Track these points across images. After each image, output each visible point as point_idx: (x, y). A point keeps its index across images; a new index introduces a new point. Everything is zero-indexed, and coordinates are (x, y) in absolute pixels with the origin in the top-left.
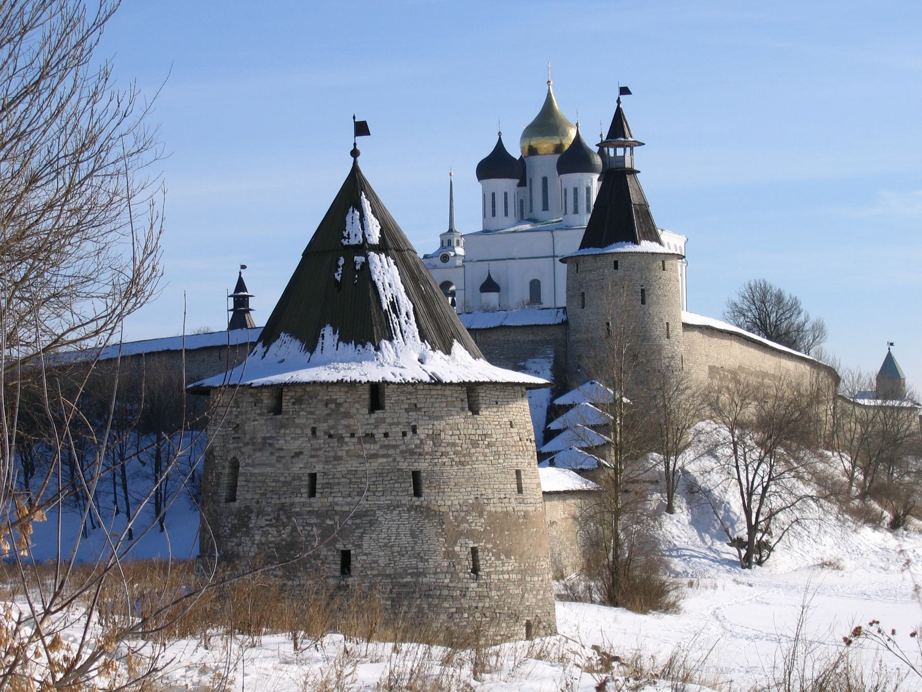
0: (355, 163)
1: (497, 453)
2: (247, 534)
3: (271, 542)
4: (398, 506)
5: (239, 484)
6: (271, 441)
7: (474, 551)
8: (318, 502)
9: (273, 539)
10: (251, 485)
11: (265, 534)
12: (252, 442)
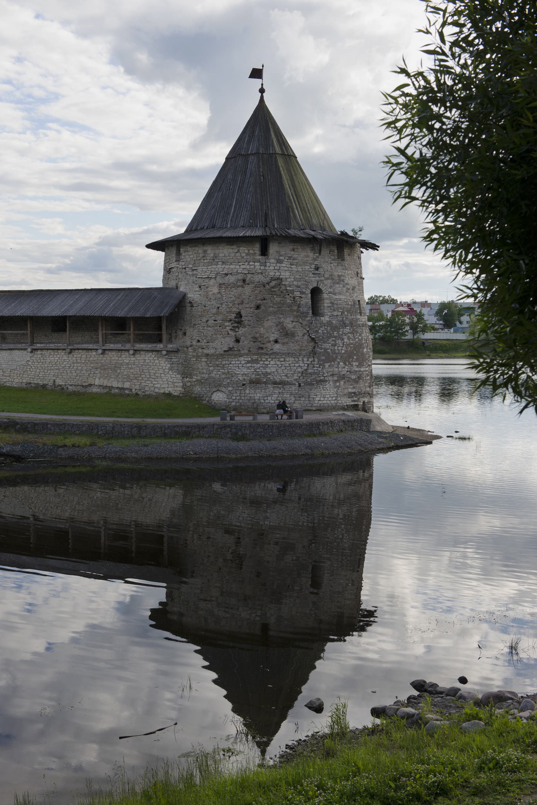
0: (262, 97)
3: (352, 344)
6: (342, 278)
11: (349, 338)
12: (331, 277)
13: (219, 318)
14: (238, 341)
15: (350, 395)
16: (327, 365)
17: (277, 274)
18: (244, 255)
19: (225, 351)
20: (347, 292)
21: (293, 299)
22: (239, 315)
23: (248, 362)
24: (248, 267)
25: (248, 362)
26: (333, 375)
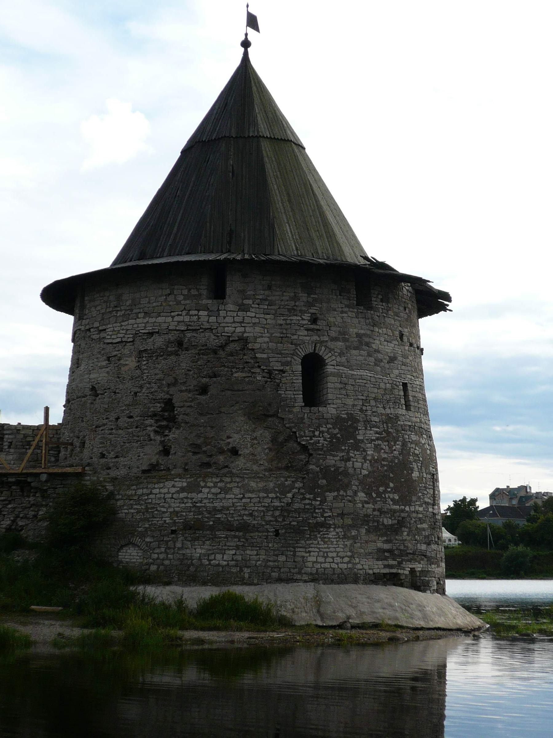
0: (246, 54)
2: (357, 446)
3: (384, 459)
6: (367, 339)
9: (386, 456)
11: (377, 448)
12: (343, 336)
13: (136, 411)
14: (166, 452)
15: (380, 555)
16: (330, 496)
17: (239, 330)
18: (181, 297)
19: (144, 472)
20: (376, 365)
21: (267, 375)
22: (169, 404)
23: (183, 490)
24: (187, 319)
25: (183, 490)
26: (342, 515)
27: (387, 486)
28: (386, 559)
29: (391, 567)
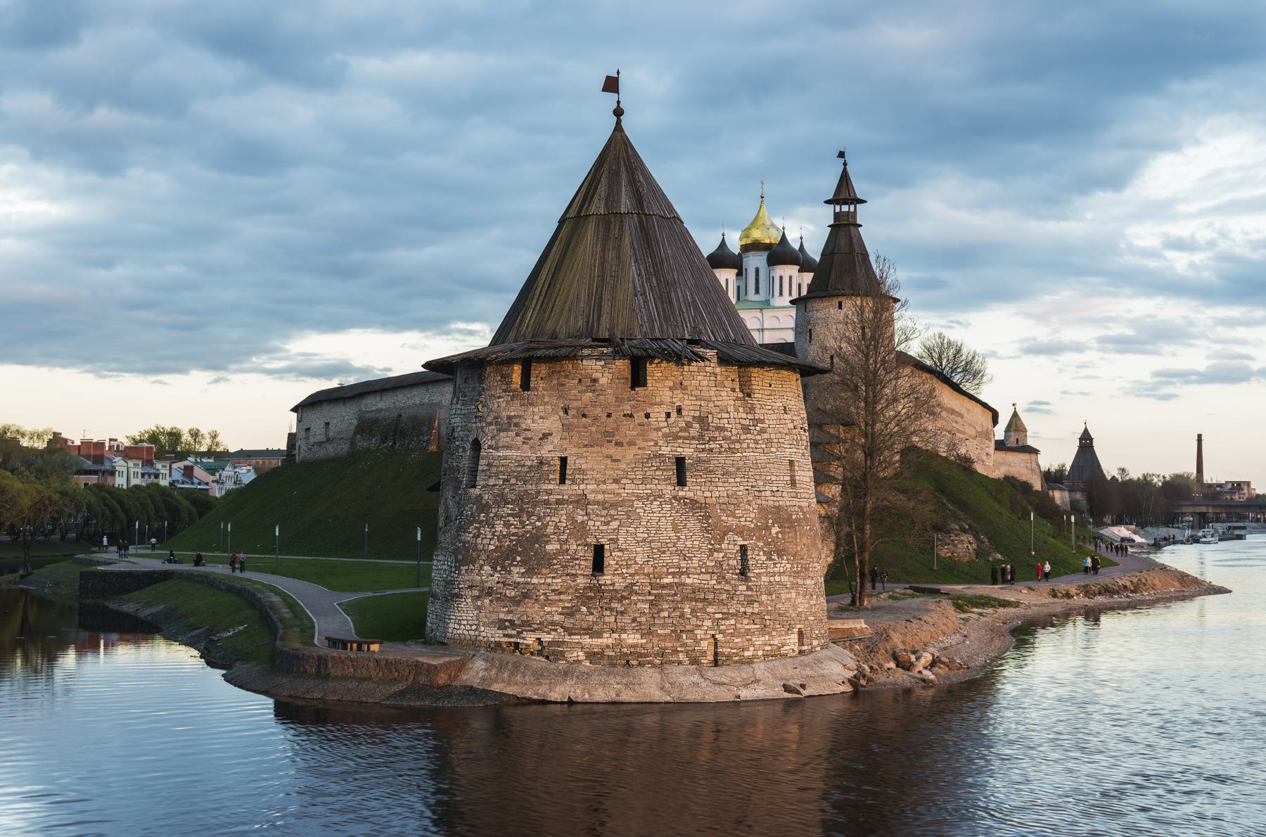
0: (619, 123)
1: (769, 441)
4: (660, 497)
5: (480, 468)
7: (743, 549)
8: (569, 489)
10: (494, 470)
15: (501, 624)
26: (471, 587)
27: (514, 560)
28: (506, 628)
29: (511, 636)
